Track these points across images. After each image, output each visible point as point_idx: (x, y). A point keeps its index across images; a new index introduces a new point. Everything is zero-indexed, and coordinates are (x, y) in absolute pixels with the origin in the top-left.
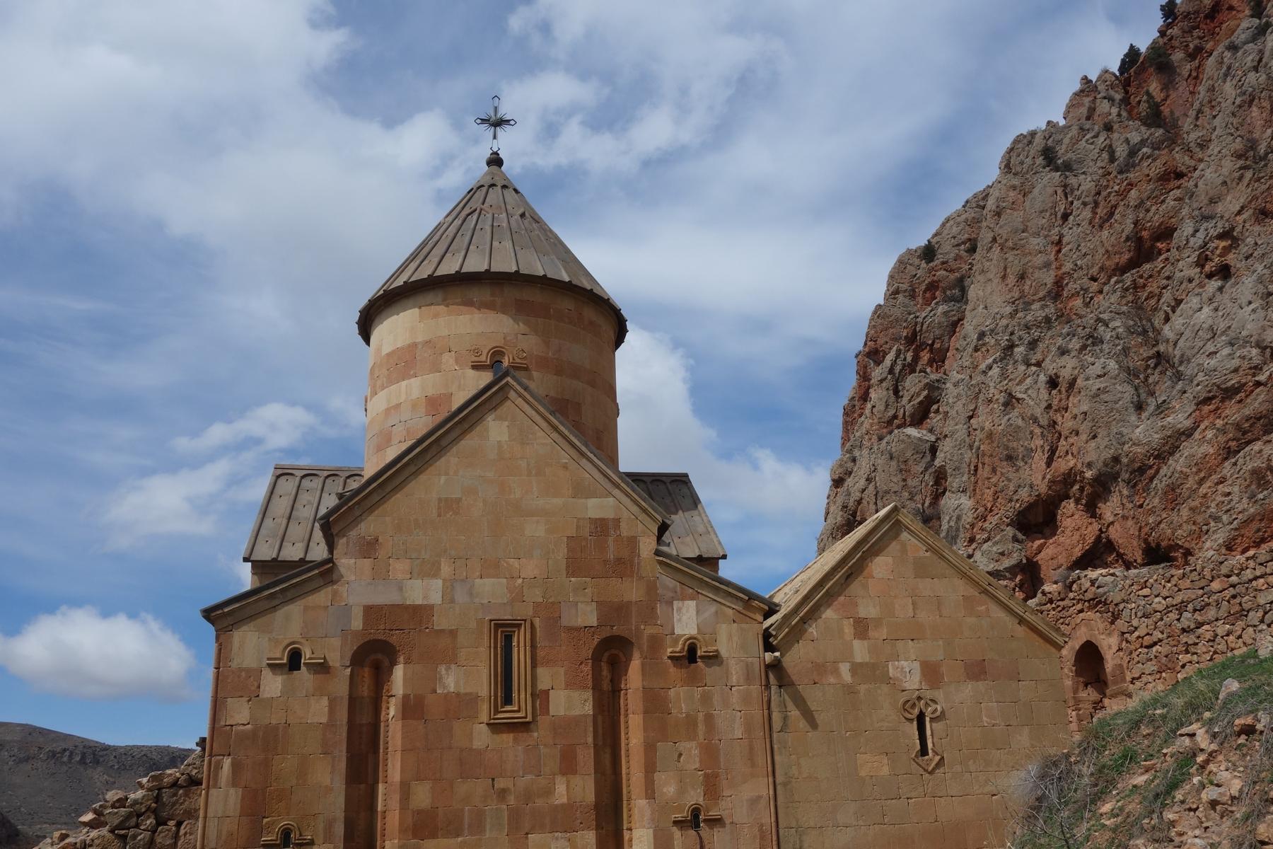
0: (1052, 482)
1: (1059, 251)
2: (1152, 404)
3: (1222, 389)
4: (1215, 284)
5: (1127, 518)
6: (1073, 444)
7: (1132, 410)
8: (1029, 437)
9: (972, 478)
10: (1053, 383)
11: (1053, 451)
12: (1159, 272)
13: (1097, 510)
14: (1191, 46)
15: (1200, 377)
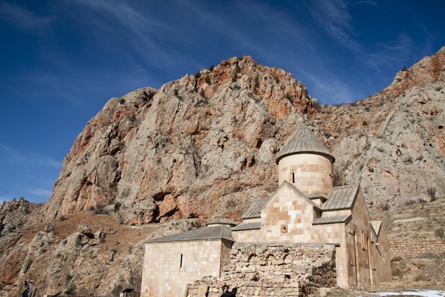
1: (173, 121)
2: (200, 175)
4: (220, 149)
7: (195, 175)
9: (142, 180)
10: (175, 161)
12: (201, 139)
14: (215, 80)
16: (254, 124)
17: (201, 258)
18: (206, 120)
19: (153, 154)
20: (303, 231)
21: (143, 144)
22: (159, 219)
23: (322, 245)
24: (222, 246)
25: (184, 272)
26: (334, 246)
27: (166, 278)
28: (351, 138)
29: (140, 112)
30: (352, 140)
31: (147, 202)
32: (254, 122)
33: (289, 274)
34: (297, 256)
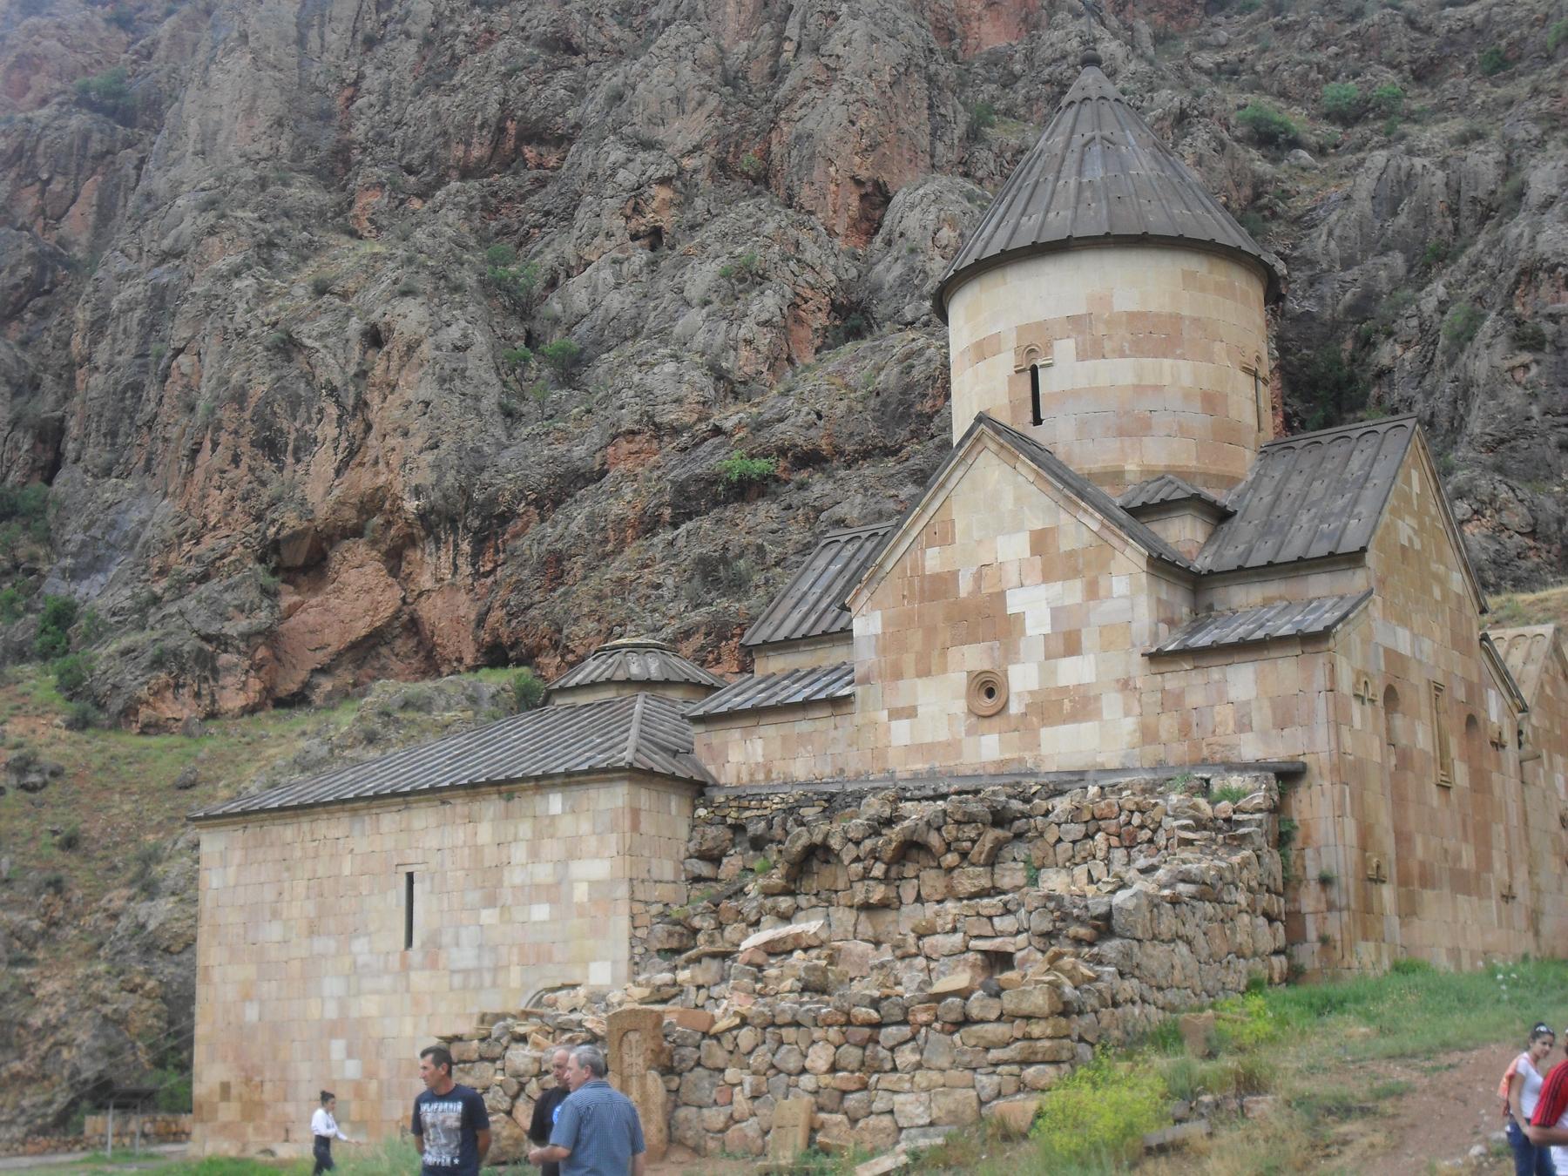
0: (341, 503)
1: (351, 100)
3: (654, 424)
5: (459, 590)
6: (393, 449)
7: (499, 418)
8: (315, 417)
10: (375, 338)
11: (352, 453)
13: (404, 564)
15: (627, 394)
16: (837, 92)
17: (522, 887)
18: (545, 83)
19: (242, 306)
20: (1097, 698)
21: (180, 247)
22: (307, 686)
23: (1206, 776)
24: (635, 813)
25: (427, 973)
26: (1271, 775)
27: (331, 1012)
28: (1410, 152)
29: (149, 56)
30: (1418, 162)
31: (226, 589)
32: (834, 79)
33: (1011, 949)
34: (1060, 847)
